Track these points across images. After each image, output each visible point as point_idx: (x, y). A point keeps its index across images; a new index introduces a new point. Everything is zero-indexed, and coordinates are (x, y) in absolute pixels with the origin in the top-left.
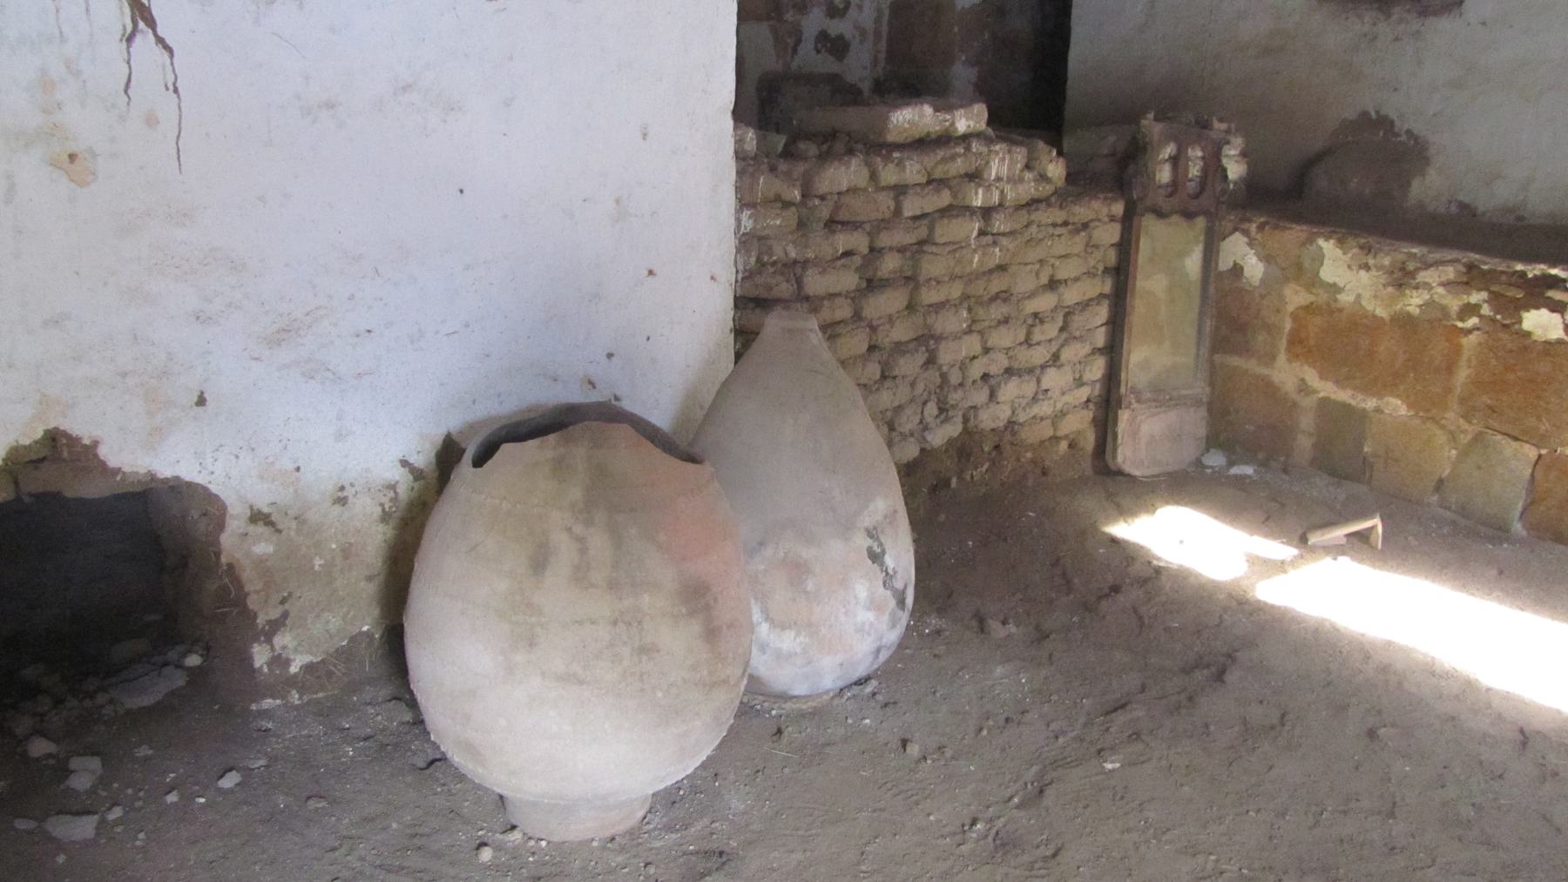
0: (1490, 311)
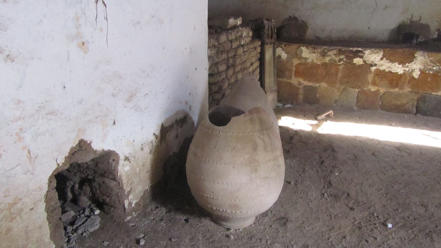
0: (346, 60)
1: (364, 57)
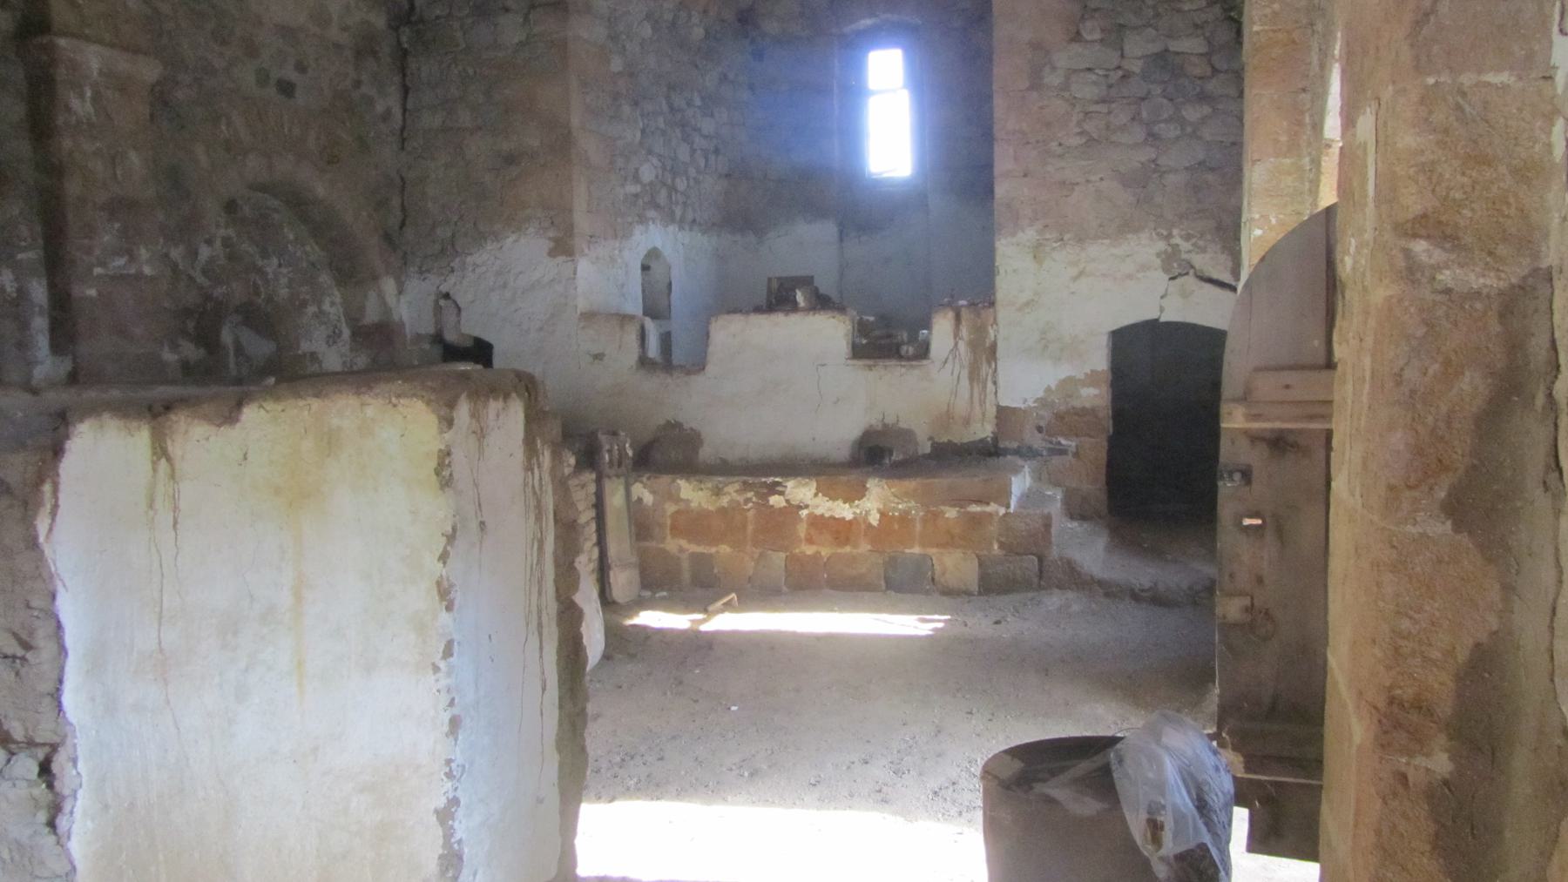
1: (787, 493)
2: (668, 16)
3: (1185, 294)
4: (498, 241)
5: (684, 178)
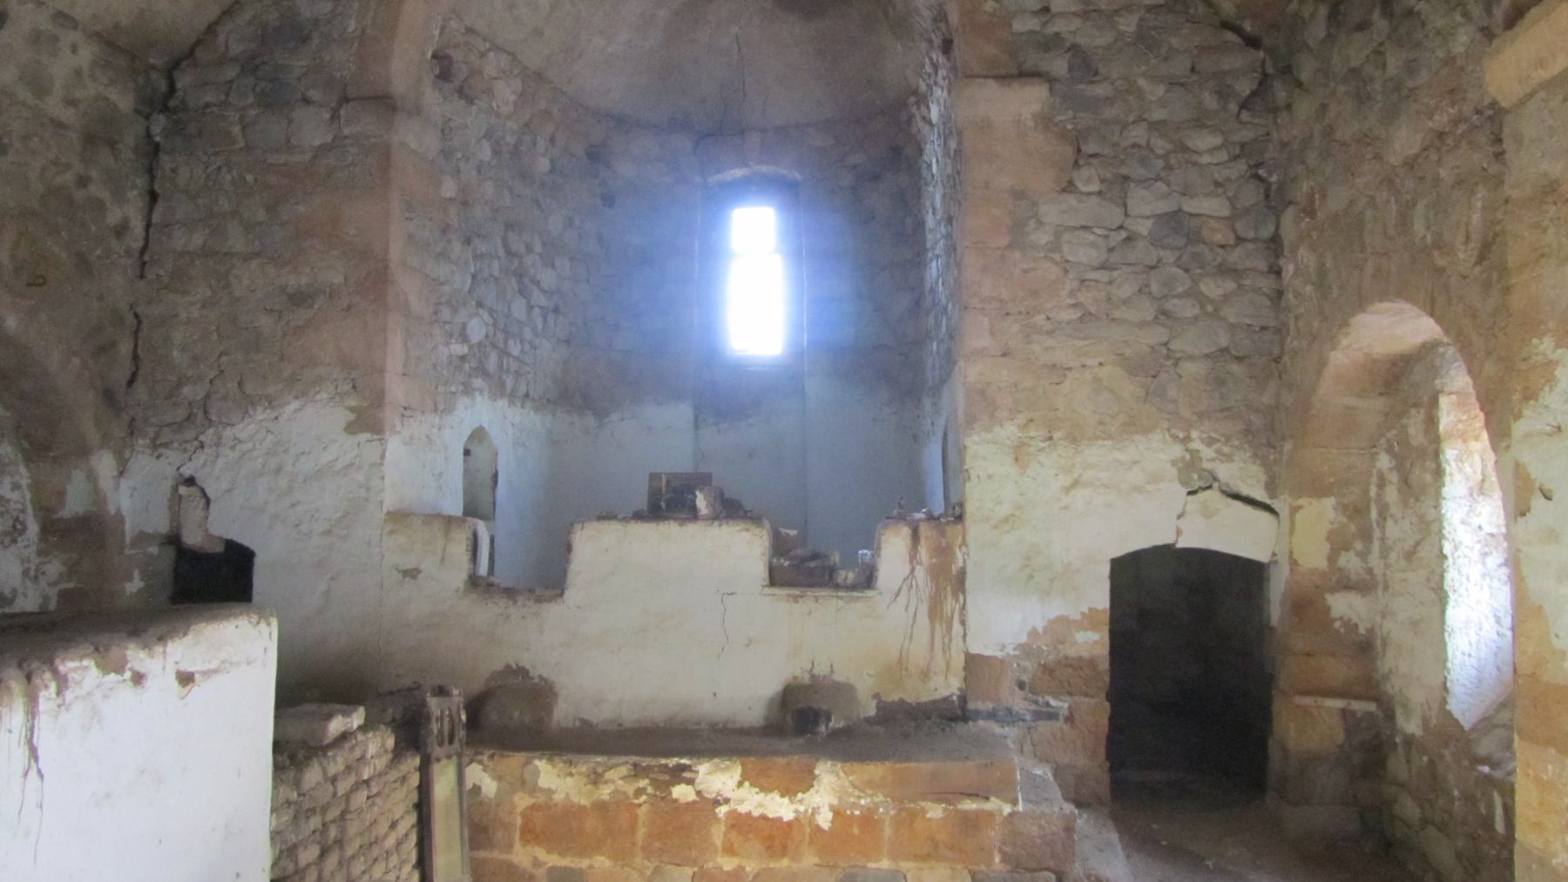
1: (697, 781)
2: (510, 139)
3: (1207, 513)
4: (273, 408)
5: (518, 341)
